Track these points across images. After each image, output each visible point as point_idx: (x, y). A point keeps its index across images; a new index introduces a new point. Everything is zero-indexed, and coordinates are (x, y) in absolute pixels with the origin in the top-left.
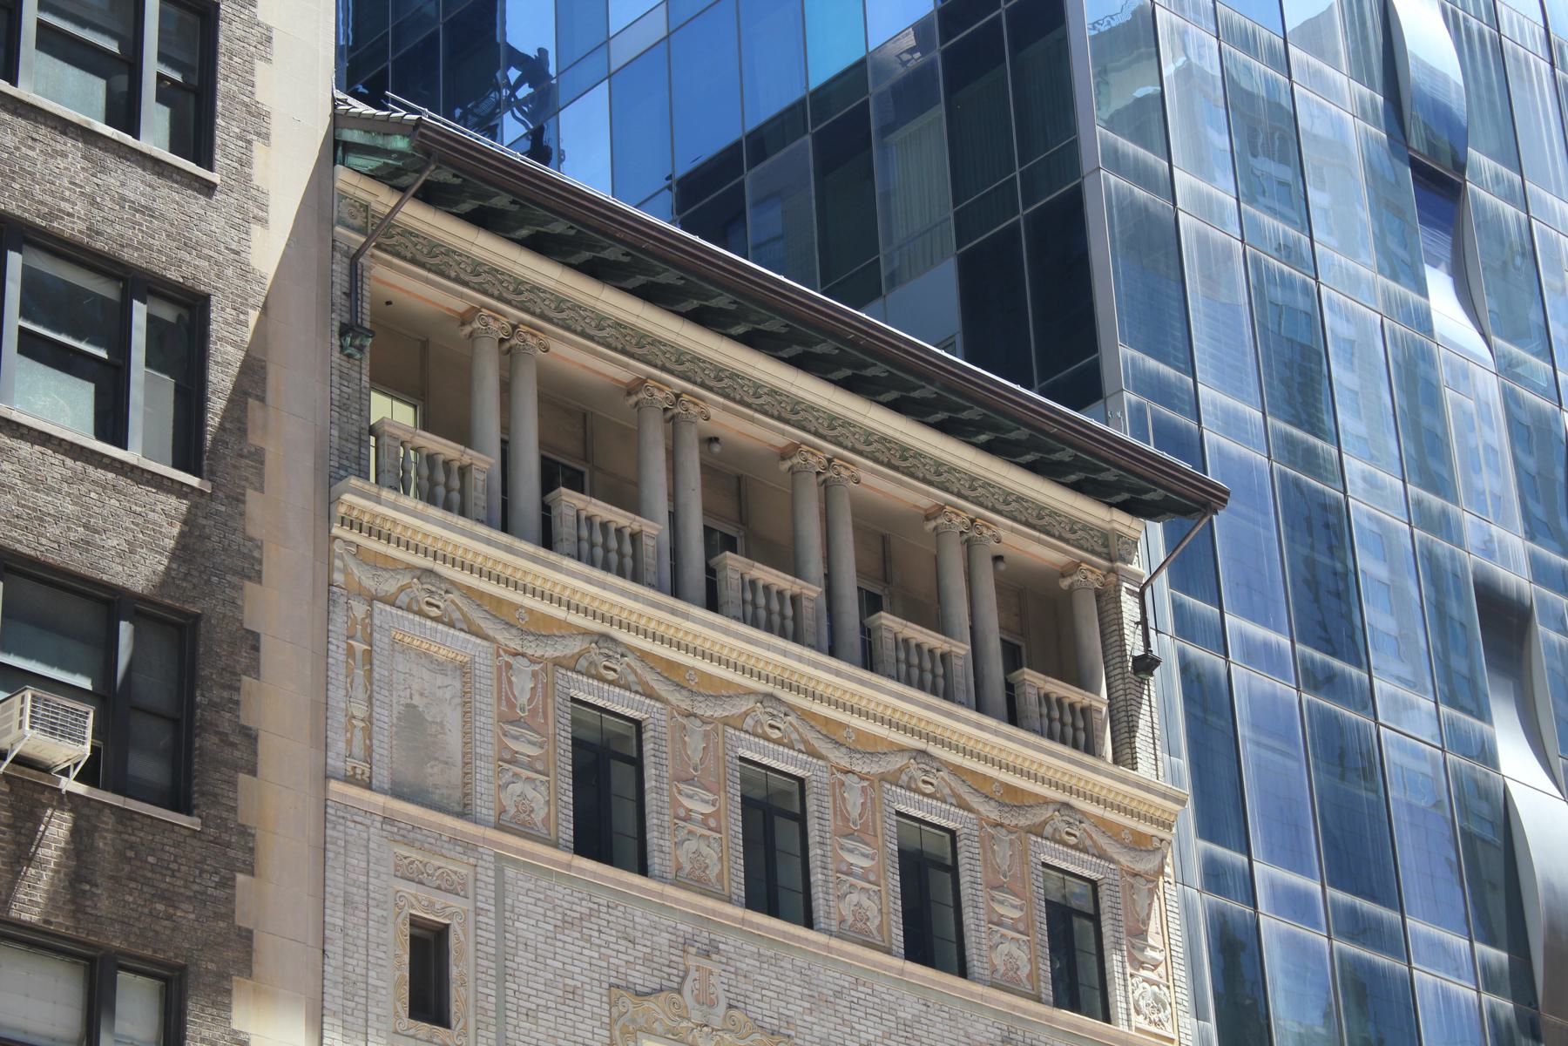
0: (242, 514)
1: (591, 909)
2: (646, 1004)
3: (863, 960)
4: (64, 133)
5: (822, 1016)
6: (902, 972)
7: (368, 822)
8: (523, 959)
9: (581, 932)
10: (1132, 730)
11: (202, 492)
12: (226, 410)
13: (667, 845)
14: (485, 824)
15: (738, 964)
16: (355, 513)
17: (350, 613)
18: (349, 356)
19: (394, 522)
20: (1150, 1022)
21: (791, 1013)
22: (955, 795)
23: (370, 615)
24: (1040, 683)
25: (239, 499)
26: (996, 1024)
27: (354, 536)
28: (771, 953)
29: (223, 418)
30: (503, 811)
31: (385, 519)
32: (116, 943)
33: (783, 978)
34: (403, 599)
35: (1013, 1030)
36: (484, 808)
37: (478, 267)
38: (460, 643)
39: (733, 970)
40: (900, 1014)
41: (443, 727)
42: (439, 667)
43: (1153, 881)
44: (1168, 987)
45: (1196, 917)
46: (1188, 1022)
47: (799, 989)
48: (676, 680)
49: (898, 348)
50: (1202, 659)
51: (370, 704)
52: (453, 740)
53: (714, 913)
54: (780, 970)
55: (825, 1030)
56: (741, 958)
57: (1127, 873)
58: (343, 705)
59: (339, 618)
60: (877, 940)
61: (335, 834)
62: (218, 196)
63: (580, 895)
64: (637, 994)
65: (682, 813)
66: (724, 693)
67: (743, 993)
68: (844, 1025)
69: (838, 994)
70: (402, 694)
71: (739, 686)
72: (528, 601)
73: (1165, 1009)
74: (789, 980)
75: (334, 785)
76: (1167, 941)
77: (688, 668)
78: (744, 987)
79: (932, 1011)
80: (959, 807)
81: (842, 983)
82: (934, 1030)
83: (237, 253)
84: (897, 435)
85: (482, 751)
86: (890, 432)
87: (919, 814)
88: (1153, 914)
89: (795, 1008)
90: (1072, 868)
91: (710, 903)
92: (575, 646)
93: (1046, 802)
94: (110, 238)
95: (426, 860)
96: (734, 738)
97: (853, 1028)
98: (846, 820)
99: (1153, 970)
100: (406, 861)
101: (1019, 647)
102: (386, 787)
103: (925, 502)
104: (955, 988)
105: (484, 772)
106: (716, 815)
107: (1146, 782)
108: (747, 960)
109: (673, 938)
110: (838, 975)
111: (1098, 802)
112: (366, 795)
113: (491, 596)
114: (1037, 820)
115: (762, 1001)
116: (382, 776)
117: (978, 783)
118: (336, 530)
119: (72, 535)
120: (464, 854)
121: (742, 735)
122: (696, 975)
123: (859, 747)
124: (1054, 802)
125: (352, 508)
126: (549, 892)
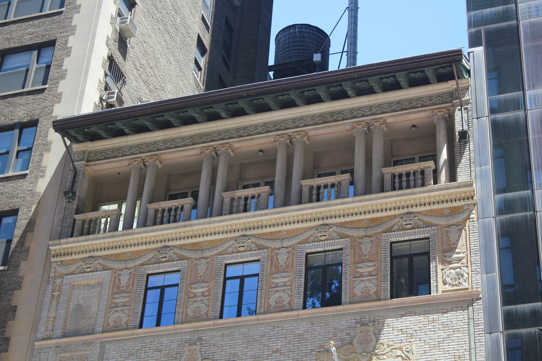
1: (142, 346)
5: (253, 347)
6: (298, 315)
7: (49, 350)
9: (136, 356)
11: (4, 270)
12: (19, 242)
14: (99, 333)
15: (211, 342)
17: (55, 284)
18: (69, 202)
19: (72, 248)
20: (453, 285)
21: (237, 351)
22: (339, 234)
23: (62, 282)
25: (18, 266)
26: (353, 319)
27: (59, 259)
29: (17, 244)
31: (68, 248)
33: (234, 339)
34: (78, 270)
35: (363, 317)
36: (99, 328)
37: (130, 147)
38: (86, 277)
39: (208, 345)
40: (296, 332)
41: (90, 306)
42: (93, 286)
43: (462, 225)
44: (467, 267)
45: (490, 230)
47: (242, 341)
48: (197, 248)
49: (267, 87)
50: (508, 117)
51: (56, 311)
53: (200, 327)
54: (233, 337)
55: (253, 352)
56: (213, 339)
58: (46, 316)
59: (50, 288)
60: (288, 307)
61: (35, 359)
62: (28, 176)
63: (138, 343)
65: (192, 295)
66: (219, 244)
67: (212, 352)
68: (264, 347)
70: (75, 302)
71: (227, 238)
72: (130, 249)
73: (463, 276)
74: (237, 339)
75: (36, 343)
76: (468, 247)
77: (202, 242)
78: (213, 349)
79: (315, 325)
80: (340, 238)
81: (265, 331)
82: (315, 333)
83: (32, 190)
84: (328, 110)
85: (102, 308)
86: (325, 110)
88: (461, 239)
89: (239, 349)
91: (198, 324)
92: (150, 256)
93: (395, 216)
95: (73, 354)
96: (221, 258)
97: (269, 346)
98: (277, 266)
99: (458, 263)
100: (64, 358)
101: (394, 161)
102: (59, 336)
103: (348, 127)
104: (328, 312)
105: (102, 315)
106: (208, 291)
107: (466, 183)
108: (216, 339)
109: (180, 343)
110: (264, 328)
111: (425, 205)
112: (49, 342)
113: (116, 254)
114: (388, 226)
115: (222, 351)
116: (59, 332)
117: (353, 225)
118: (53, 260)
120: (88, 347)
121: (225, 256)
122: (188, 353)
124: (399, 215)
125: (55, 250)
126: (124, 347)
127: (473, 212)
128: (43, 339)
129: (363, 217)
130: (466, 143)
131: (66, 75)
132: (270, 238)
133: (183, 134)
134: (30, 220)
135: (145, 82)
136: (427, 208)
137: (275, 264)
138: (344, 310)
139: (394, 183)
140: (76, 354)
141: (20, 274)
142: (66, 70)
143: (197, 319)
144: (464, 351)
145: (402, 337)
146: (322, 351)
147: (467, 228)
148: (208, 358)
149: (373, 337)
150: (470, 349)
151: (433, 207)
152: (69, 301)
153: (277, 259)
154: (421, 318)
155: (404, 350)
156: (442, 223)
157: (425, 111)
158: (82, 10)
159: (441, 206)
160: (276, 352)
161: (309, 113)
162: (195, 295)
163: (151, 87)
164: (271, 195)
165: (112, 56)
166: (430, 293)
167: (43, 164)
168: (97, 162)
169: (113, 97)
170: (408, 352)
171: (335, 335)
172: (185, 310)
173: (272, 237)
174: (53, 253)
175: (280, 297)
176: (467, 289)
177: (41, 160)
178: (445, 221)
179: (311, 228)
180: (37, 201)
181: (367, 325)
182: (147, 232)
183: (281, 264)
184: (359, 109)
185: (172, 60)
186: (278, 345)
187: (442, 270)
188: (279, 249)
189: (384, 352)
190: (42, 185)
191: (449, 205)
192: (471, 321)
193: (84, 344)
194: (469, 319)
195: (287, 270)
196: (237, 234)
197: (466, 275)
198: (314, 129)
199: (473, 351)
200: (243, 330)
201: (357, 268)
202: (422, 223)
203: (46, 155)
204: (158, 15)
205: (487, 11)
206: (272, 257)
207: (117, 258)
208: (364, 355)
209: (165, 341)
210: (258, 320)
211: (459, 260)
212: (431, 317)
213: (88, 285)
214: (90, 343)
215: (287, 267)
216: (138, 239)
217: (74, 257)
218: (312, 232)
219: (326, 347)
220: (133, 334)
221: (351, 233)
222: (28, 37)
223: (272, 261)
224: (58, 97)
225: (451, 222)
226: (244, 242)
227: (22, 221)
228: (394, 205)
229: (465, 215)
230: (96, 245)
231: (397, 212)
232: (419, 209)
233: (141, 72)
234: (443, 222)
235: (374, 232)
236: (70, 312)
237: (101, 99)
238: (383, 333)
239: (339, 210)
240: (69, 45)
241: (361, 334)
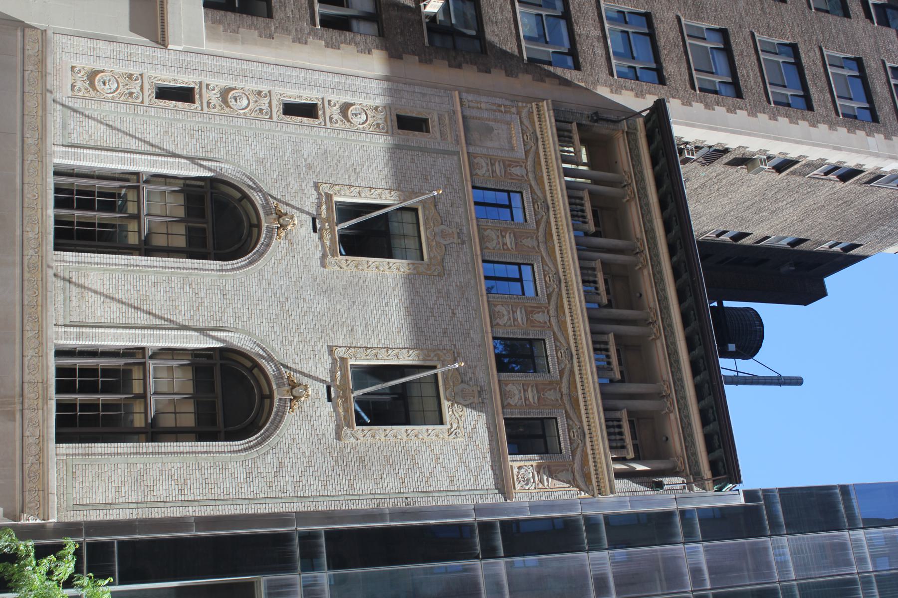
2: (433, 208)
3: (484, 312)
4: (602, 31)
6: (487, 333)
11: (523, 59)
12: (550, 72)
14: (467, 149)
16: (541, 108)
18: (588, 117)
19: (545, 121)
20: (517, 476)
23: (514, 114)
24: (624, 420)
25: (527, 72)
27: (535, 110)
28: (471, 269)
29: (548, 71)
30: (475, 158)
31: (545, 117)
32: (384, 16)
34: (525, 128)
37: (641, 172)
41: (492, 140)
44: (535, 488)
45: (570, 510)
50: (677, 527)
51: (487, 110)
53: (475, 242)
57: (572, 468)
58: (482, 100)
59: (508, 103)
60: (494, 323)
62: (611, 78)
64: (435, 206)
65: (503, 234)
69: (467, 299)
71: (557, 265)
73: (527, 484)
75: (457, 93)
76: (554, 490)
77: (553, 241)
80: (559, 371)
84: (681, 358)
86: (680, 355)
87: (549, 354)
88: (561, 483)
90: (562, 439)
91: (477, 240)
93: (581, 422)
94: (580, 41)
98: (532, 312)
101: (633, 420)
103: (665, 377)
104: (491, 361)
112: (458, 104)
114: (571, 415)
116: (468, 113)
117: (572, 384)
118: (534, 104)
119: (492, 17)
122: (450, 232)
123: (560, 322)
124: (582, 426)
125: (543, 106)
127: (587, 495)
128: (461, 99)
129: (580, 392)
130: (652, 488)
131: (709, 109)
132: (559, 305)
133: (655, 221)
134: (571, 81)
135: (704, 184)
136: (590, 452)
137: (534, 311)
138: (493, 375)
139: (612, 421)
140: (448, 130)
141: (520, 75)
142: (714, 109)
143: (482, 239)
144: (458, 485)
145: (469, 429)
146: (454, 355)
147: (571, 488)
148: (446, 250)
149: (468, 402)
150: (460, 491)
151: (590, 457)
152: (496, 121)
153: (539, 312)
154: (487, 446)
155: (457, 430)
156: (576, 465)
157: (682, 449)
158: (773, 122)
159: (591, 464)
160: (453, 313)
161: (678, 340)
162: (504, 237)
163: (700, 190)
164: (599, 305)
165: (729, 152)
166: (509, 454)
167: (624, 92)
168: (626, 141)
169: (689, 154)
170: (456, 434)
171: (469, 367)
172: (490, 227)
173: (559, 308)
174: (540, 104)
175: (503, 315)
176: (515, 488)
177: (627, 90)
178: (578, 468)
179: (568, 344)
180: (588, 87)
181: (480, 396)
182: (562, 190)
183: (535, 316)
184: (683, 387)
185: (727, 209)
186: (460, 314)
187: (532, 466)
188: (548, 313)
189: (455, 412)
190: (603, 91)
191: (593, 472)
192: (485, 492)
193: (457, 136)
194: (487, 490)
195: (529, 321)
196: (561, 274)
197: (527, 487)
198: (662, 345)
199: (458, 493)
200: (472, 282)
201: (532, 387)
202: (575, 447)
203: (632, 94)
204: (770, 195)
205: (779, 508)
206: (540, 308)
207: (537, 163)
208: (451, 394)
209: (461, 210)
210: (482, 295)
211: (541, 482)
212: (488, 455)
213: (511, 138)
214: (458, 142)
215: (532, 321)
216: (555, 182)
217: (537, 124)
218: (565, 345)
219: (459, 358)
220: (466, 180)
221: (565, 380)
222: (745, 72)
223: (537, 308)
224: (687, 103)
225: (576, 474)
226: (554, 281)
227: (570, 75)
228: (592, 420)
229: (583, 486)
230: (548, 144)
231: (585, 424)
232: (588, 444)
233: (713, 180)
234: (576, 466)
235: (566, 402)
236: (486, 122)
237: (687, 143)
238: (473, 411)
239: (586, 369)
240: (738, 111)
241: (471, 391)
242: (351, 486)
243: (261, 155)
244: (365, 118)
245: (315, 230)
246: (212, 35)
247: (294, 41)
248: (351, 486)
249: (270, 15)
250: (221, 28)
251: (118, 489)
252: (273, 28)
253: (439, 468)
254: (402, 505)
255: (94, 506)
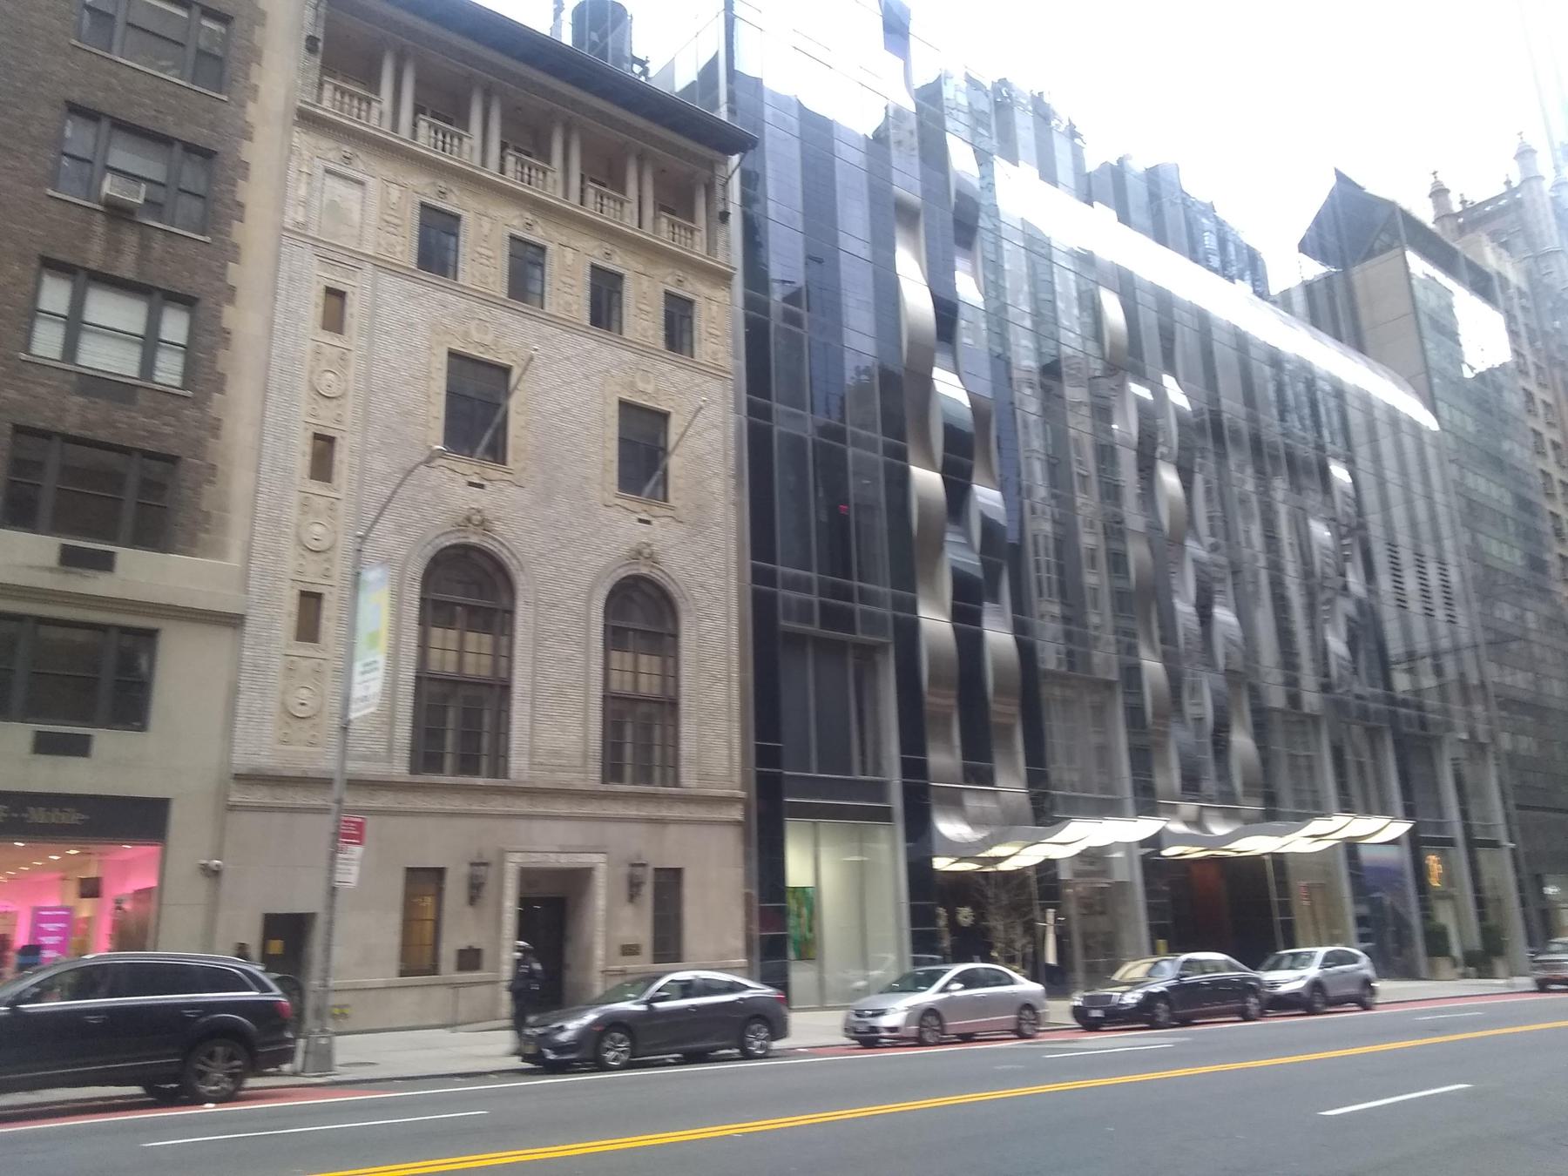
0: (245, 113)
8: (384, 311)
10: (716, 243)
13: (467, 268)
25: (242, 106)
46: (730, 359)
52: (356, 217)
160: (568, 359)
242: (717, 525)
243: (391, 526)
244: (332, 375)
245: (481, 486)
246: (218, 551)
247: (216, 437)
248: (717, 525)
249: (172, 460)
250: (203, 535)
251: (718, 736)
252: (197, 461)
253: (705, 435)
254: (732, 482)
255: (730, 757)
